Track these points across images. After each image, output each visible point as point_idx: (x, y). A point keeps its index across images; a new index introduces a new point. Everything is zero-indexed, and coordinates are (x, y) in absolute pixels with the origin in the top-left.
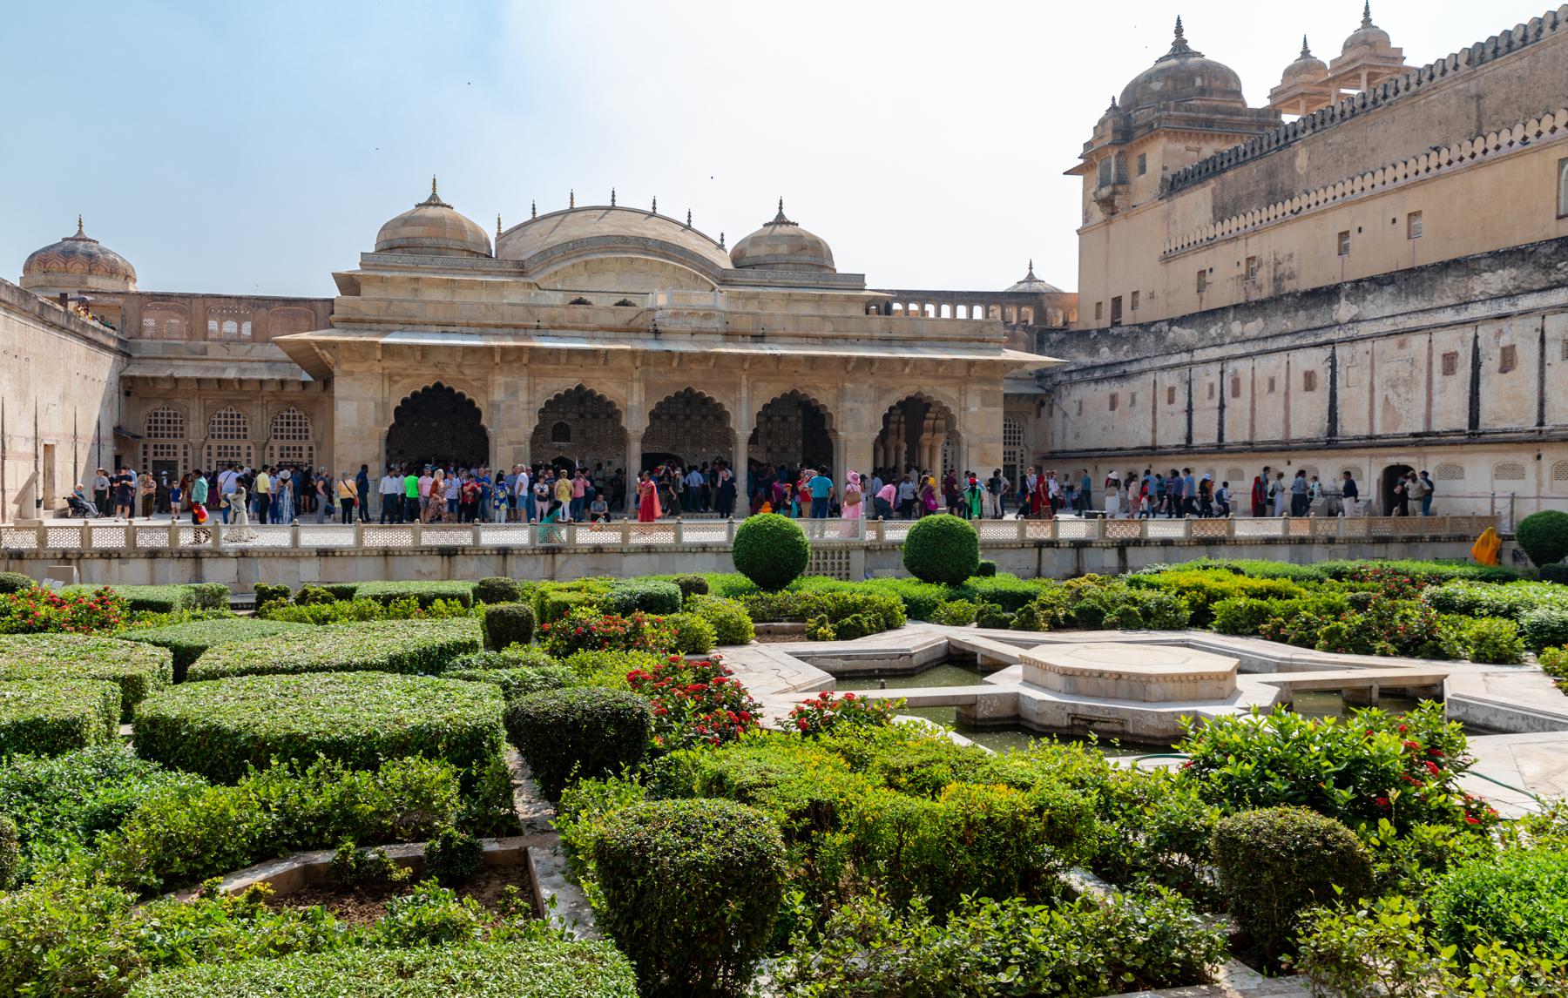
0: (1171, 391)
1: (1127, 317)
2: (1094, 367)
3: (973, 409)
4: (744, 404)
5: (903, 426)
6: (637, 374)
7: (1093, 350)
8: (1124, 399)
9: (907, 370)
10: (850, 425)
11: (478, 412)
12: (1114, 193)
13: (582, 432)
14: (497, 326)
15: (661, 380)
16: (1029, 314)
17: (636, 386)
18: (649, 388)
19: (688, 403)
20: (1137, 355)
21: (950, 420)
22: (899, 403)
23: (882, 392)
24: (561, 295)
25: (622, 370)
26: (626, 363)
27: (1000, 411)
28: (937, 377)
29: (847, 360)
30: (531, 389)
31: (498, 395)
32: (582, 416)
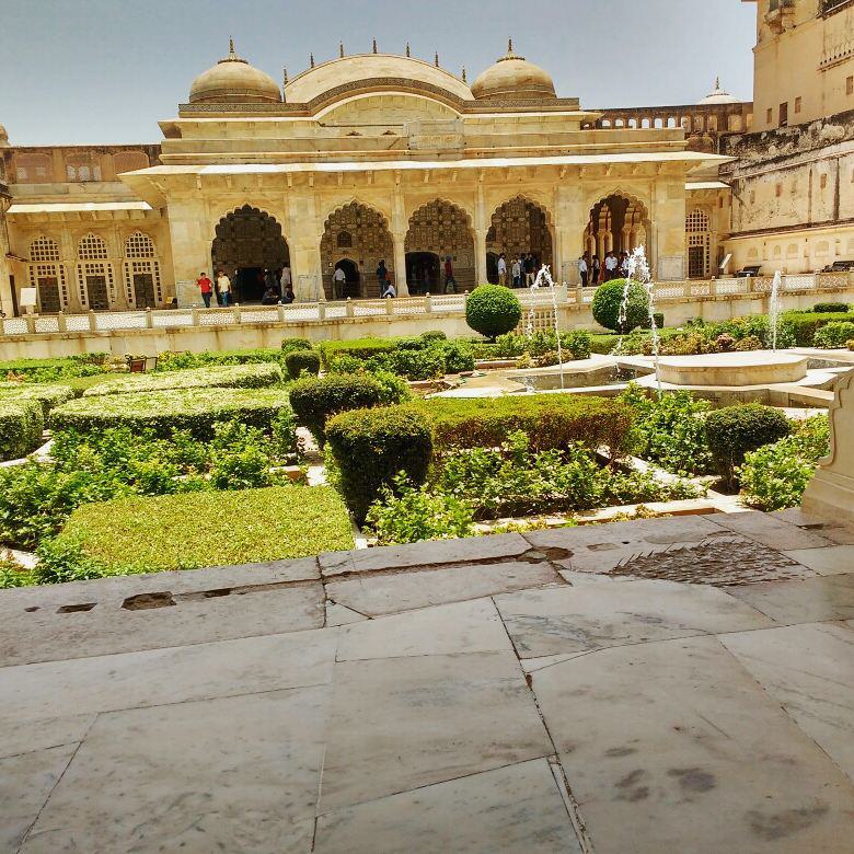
0: (824, 177)
1: (792, 118)
3: (662, 201)
4: (481, 206)
5: (610, 220)
6: (398, 189)
7: (764, 148)
8: (787, 187)
9: (608, 173)
10: (563, 220)
11: (279, 226)
12: (781, 14)
13: (360, 239)
15: (417, 193)
16: (713, 120)
17: (397, 198)
18: (408, 201)
19: (440, 211)
20: (798, 150)
21: (644, 213)
22: (603, 202)
23: (590, 192)
25: (385, 186)
26: (388, 180)
27: (682, 202)
28: (632, 177)
29: (560, 168)
30: (318, 206)
31: (293, 211)
32: (359, 226)
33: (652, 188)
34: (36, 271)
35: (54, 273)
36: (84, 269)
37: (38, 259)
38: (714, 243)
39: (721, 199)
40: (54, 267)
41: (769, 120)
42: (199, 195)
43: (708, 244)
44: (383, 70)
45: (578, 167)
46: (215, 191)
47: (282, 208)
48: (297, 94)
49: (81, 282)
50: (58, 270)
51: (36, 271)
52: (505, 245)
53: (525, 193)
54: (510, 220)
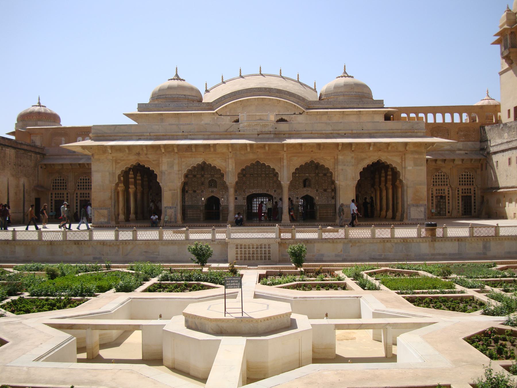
2: (502, 144)
3: (409, 168)
4: (285, 169)
6: (231, 155)
9: (371, 149)
11: (156, 175)
12: (510, 53)
14: (163, 135)
17: (230, 160)
24: (229, 118)
25: (223, 153)
26: (225, 150)
27: (424, 168)
29: (337, 144)
31: (164, 167)
33: (403, 159)
34: (54, 196)
35: (63, 197)
36: (79, 195)
37: (56, 189)
38: (478, 193)
39: (482, 165)
40: (63, 194)
41: (509, 117)
42: (110, 157)
43: (475, 193)
44: (260, 83)
45: (351, 144)
46: (119, 155)
47: (158, 165)
48: (207, 98)
49: (77, 203)
50: (65, 195)
51: (54, 196)
52: (317, 191)
53: (315, 159)
54: (321, 175)
